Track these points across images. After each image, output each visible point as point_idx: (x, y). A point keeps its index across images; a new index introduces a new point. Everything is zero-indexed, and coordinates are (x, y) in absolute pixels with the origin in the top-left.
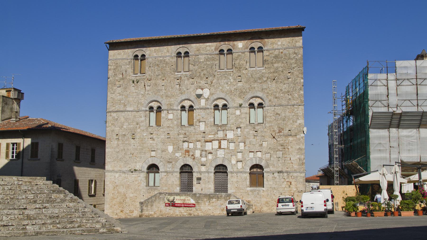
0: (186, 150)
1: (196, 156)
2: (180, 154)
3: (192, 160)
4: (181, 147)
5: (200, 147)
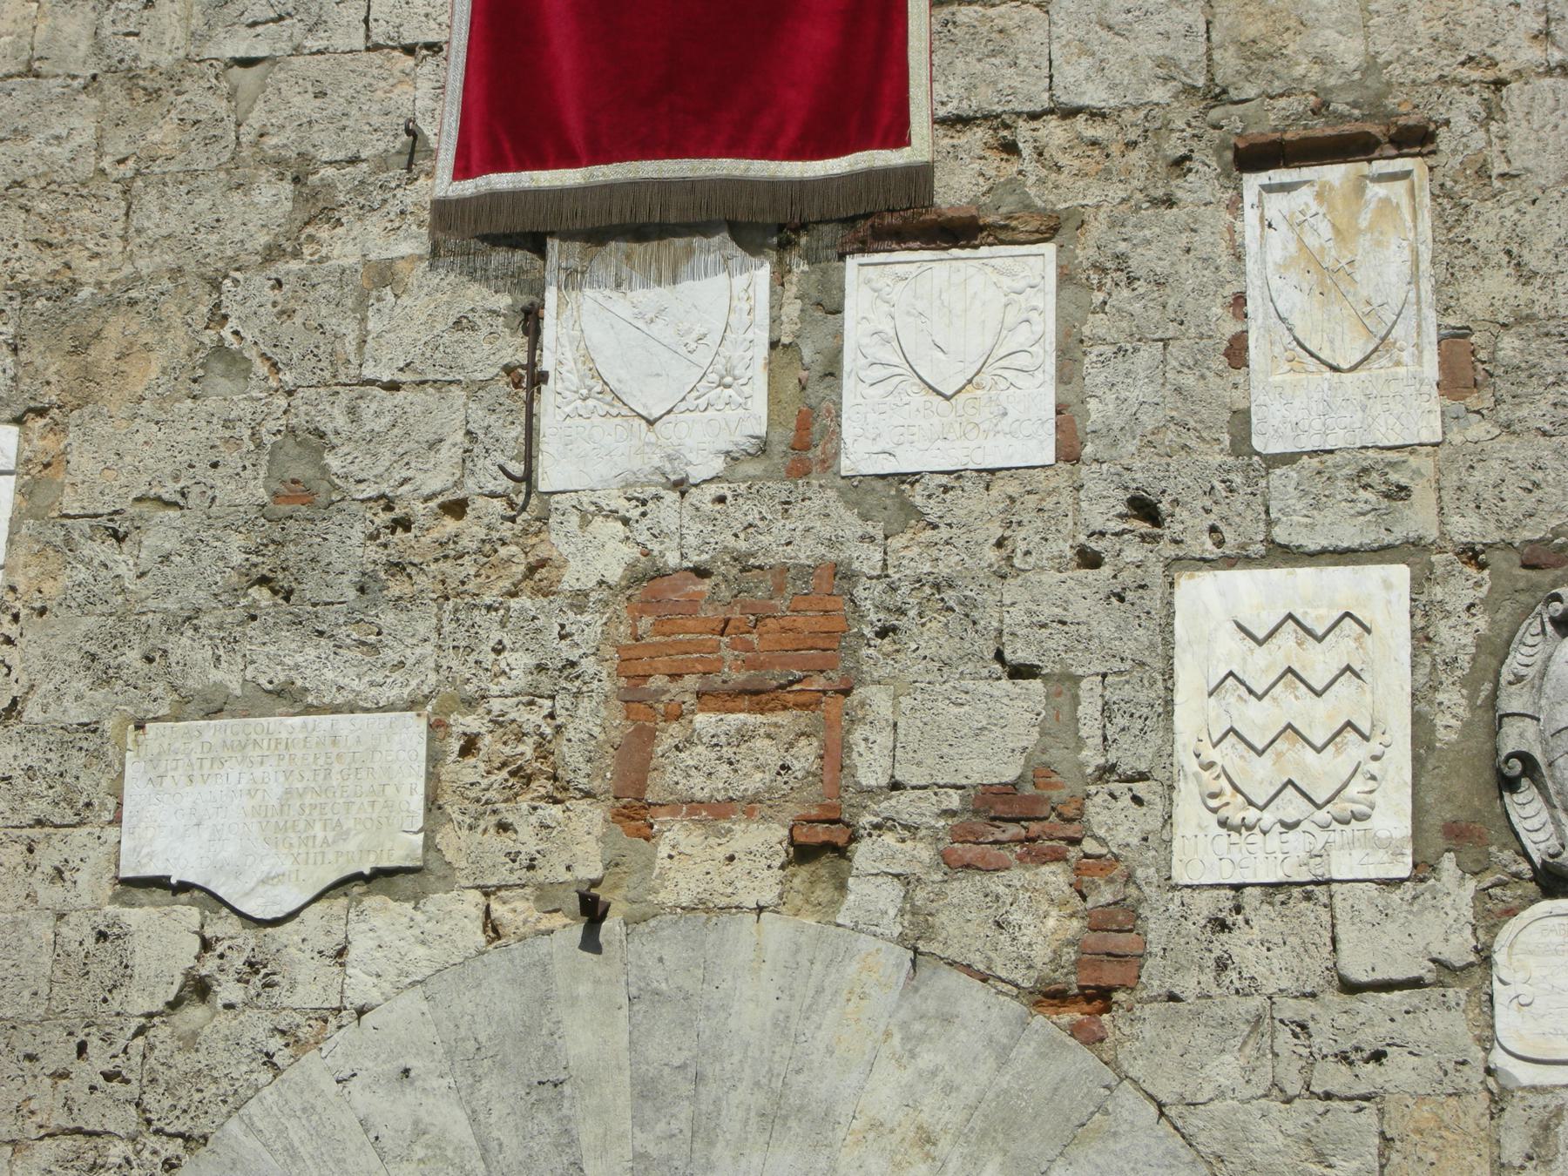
0: (647, 580)
1: (1203, 855)
2: (371, 774)
3: (985, 1044)
4: (421, 450)
5: (1404, 406)
